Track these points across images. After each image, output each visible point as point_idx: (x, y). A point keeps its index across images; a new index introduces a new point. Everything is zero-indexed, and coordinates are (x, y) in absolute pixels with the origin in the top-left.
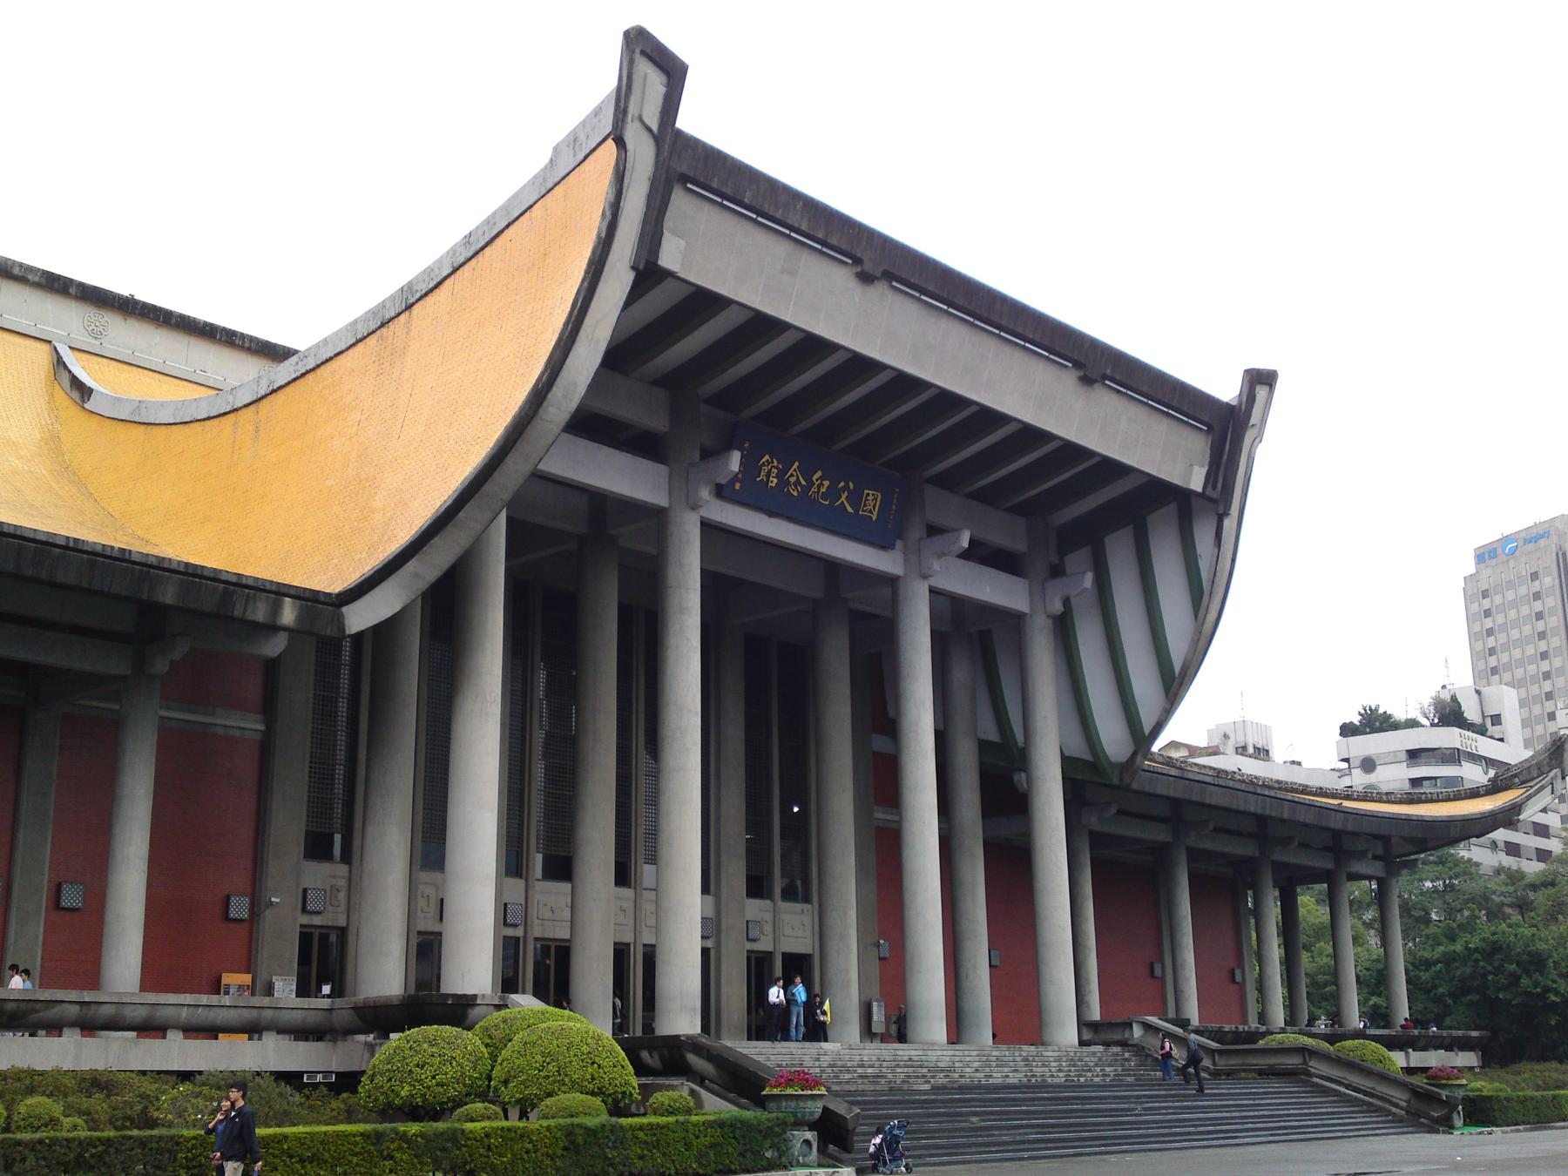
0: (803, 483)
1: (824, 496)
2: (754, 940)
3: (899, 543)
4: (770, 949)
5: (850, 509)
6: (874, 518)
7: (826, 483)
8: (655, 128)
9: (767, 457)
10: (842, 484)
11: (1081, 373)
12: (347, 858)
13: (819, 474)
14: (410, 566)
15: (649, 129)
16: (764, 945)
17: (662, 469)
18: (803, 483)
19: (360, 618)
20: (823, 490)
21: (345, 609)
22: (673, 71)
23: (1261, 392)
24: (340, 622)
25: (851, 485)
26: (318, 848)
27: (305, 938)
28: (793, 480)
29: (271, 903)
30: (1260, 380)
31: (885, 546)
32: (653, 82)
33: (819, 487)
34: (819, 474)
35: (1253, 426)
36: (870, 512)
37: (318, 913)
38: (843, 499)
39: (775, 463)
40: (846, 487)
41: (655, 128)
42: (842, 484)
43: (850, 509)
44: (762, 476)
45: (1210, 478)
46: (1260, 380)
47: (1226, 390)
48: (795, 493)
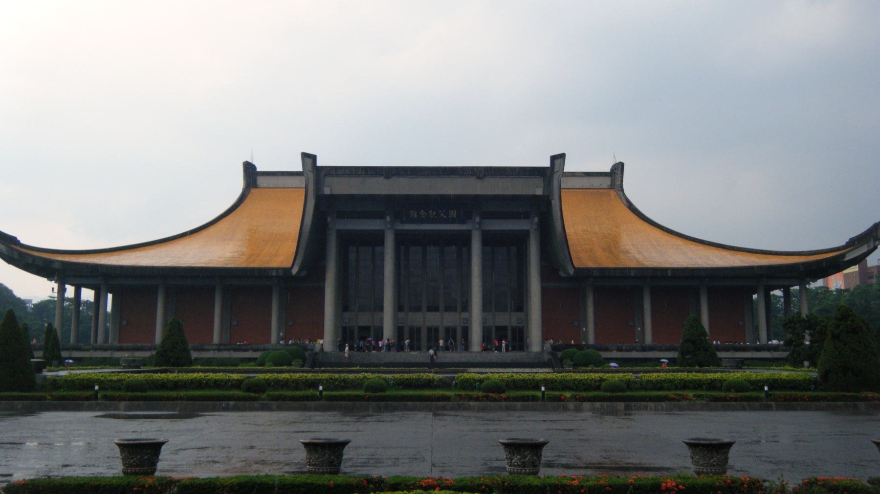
1: (434, 216)
5: (445, 217)
9: (412, 211)
11: (475, 177)
19: (295, 271)
20: (434, 214)
22: (313, 158)
23: (557, 162)
25: (444, 211)
28: (423, 214)
31: (463, 221)
34: (431, 211)
35: (557, 172)
40: (442, 212)
42: (440, 211)
43: (445, 217)
44: (412, 216)
47: (547, 164)
48: (424, 218)
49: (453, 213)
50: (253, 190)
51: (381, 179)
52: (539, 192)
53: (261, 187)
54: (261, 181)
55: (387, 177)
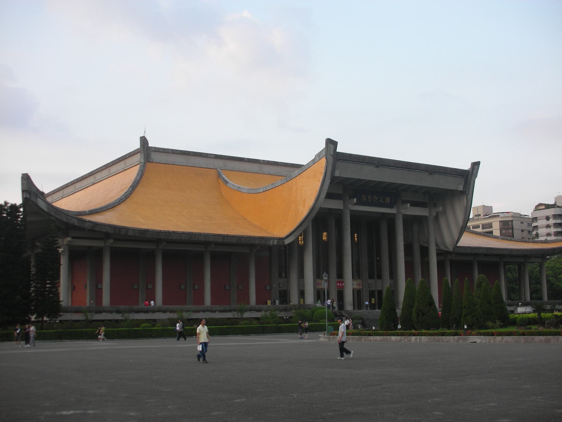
0: (371, 199)
1: (377, 200)
2: (371, 288)
3: (395, 206)
4: (374, 289)
5: (383, 202)
6: (389, 202)
7: (377, 198)
8: (332, 155)
9: (363, 195)
10: (380, 197)
12: (286, 277)
13: (375, 196)
14: (295, 233)
15: (331, 155)
16: (373, 289)
17: (341, 202)
18: (371, 199)
19: (287, 242)
20: (376, 199)
21: (284, 240)
23: (476, 167)
24: (284, 242)
26: (280, 276)
27: (280, 292)
28: (369, 199)
29: (273, 286)
30: (476, 165)
31: (391, 206)
32: (332, 147)
33: (375, 199)
34: (375, 196)
35: (474, 175)
36: (387, 201)
37: (282, 288)
38: (381, 200)
39: (365, 196)
41: (332, 155)
42: (380, 197)
43: (383, 202)
45: (464, 187)
46: (476, 165)
48: (370, 201)
49: (388, 200)
50: (148, 165)
51: (372, 168)
52: (461, 188)
53: (154, 161)
54: (155, 157)
55: (377, 167)
